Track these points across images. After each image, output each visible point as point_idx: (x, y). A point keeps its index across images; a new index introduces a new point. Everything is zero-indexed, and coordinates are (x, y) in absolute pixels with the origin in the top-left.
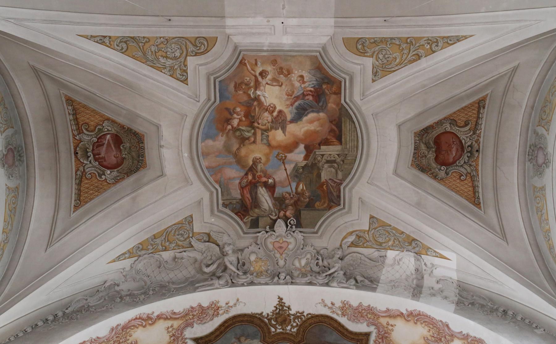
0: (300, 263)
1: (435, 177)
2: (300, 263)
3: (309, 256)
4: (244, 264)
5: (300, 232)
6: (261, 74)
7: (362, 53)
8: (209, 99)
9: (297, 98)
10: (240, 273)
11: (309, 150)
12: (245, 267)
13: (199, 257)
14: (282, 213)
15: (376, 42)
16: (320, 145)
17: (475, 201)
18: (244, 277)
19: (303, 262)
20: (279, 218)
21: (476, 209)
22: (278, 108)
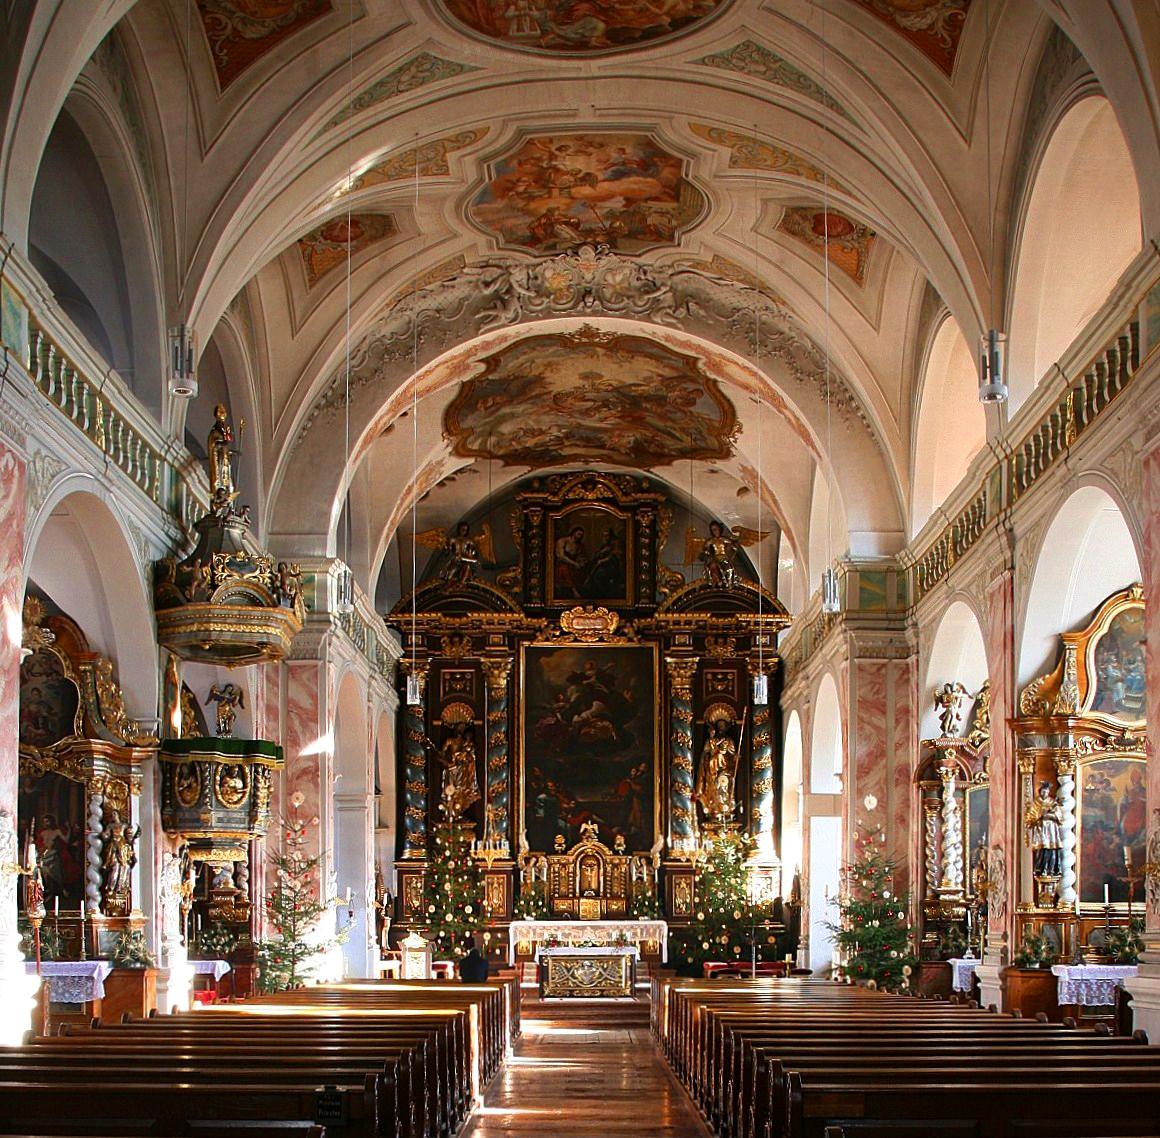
0: (614, 279)
1: (809, 242)
2: (614, 279)
3: (627, 271)
4: (536, 278)
5: (616, 254)
6: (559, 149)
7: (721, 141)
8: (482, 180)
9: (613, 165)
10: (533, 294)
11: (629, 201)
12: (539, 282)
13: (473, 279)
14: (589, 240)
15: (738, 136)
16: (646, 200)
17: (857, 276)
18: (538, 301)
19: (619, 278)
20: (585, 244)
21: (853, 284)
22: (584, 171)
